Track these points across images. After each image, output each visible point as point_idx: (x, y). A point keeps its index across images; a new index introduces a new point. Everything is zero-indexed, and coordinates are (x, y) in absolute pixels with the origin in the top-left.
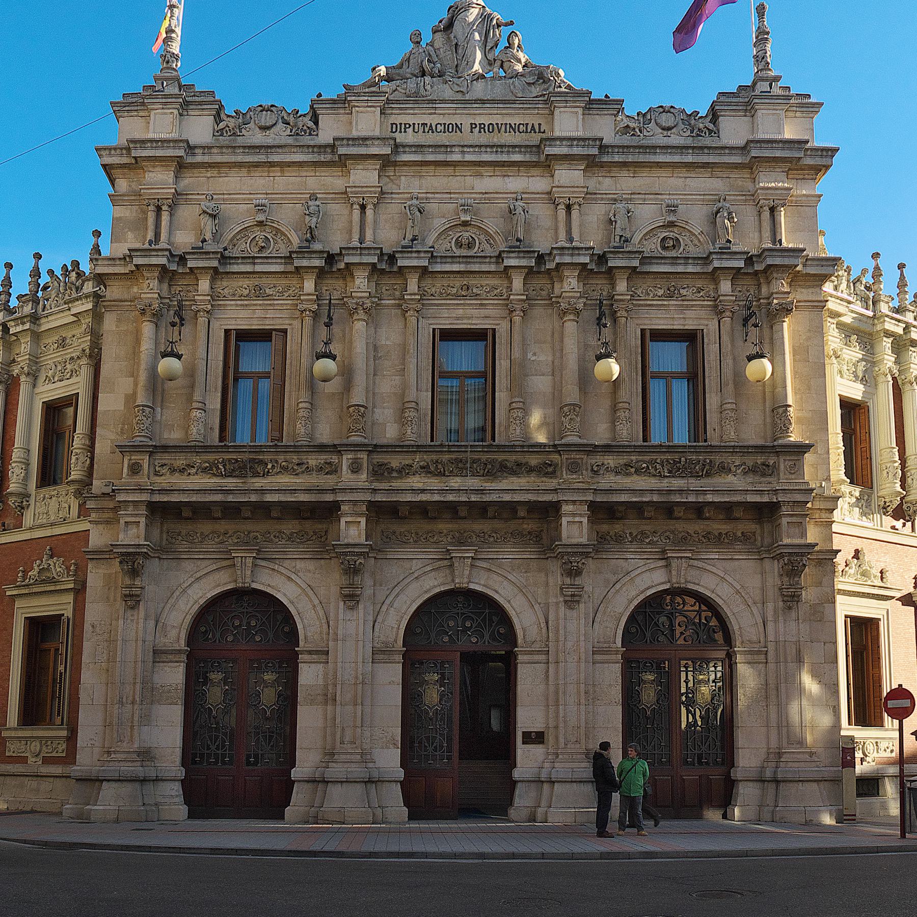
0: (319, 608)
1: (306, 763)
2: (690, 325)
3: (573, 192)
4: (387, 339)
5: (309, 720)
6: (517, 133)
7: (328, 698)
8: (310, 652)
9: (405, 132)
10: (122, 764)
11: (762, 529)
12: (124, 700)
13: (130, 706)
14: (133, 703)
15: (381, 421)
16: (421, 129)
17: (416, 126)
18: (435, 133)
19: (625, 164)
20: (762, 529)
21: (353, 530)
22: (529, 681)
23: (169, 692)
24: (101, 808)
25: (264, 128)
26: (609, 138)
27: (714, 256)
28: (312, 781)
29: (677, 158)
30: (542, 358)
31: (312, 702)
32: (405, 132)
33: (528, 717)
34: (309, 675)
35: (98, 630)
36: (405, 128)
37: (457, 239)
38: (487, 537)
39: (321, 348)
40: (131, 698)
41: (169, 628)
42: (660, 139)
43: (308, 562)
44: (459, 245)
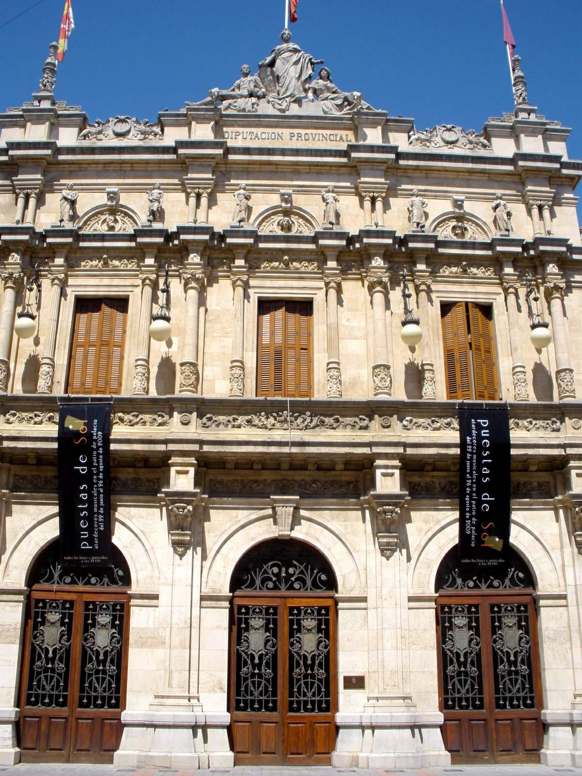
1: (137, 705)
2: (482, 299)
3: (376, 188)
4: (218, 305)
5: (141, 665)
6: (328, 141)
16: (249, 137)
17: (245, 133)
18: (260, 140)
21: (182, 481)
23: (8, 631)
25: (118, 135)
32: (235, 138)
33: (347, 664)
37: (279, 223)
39: (156, 310)
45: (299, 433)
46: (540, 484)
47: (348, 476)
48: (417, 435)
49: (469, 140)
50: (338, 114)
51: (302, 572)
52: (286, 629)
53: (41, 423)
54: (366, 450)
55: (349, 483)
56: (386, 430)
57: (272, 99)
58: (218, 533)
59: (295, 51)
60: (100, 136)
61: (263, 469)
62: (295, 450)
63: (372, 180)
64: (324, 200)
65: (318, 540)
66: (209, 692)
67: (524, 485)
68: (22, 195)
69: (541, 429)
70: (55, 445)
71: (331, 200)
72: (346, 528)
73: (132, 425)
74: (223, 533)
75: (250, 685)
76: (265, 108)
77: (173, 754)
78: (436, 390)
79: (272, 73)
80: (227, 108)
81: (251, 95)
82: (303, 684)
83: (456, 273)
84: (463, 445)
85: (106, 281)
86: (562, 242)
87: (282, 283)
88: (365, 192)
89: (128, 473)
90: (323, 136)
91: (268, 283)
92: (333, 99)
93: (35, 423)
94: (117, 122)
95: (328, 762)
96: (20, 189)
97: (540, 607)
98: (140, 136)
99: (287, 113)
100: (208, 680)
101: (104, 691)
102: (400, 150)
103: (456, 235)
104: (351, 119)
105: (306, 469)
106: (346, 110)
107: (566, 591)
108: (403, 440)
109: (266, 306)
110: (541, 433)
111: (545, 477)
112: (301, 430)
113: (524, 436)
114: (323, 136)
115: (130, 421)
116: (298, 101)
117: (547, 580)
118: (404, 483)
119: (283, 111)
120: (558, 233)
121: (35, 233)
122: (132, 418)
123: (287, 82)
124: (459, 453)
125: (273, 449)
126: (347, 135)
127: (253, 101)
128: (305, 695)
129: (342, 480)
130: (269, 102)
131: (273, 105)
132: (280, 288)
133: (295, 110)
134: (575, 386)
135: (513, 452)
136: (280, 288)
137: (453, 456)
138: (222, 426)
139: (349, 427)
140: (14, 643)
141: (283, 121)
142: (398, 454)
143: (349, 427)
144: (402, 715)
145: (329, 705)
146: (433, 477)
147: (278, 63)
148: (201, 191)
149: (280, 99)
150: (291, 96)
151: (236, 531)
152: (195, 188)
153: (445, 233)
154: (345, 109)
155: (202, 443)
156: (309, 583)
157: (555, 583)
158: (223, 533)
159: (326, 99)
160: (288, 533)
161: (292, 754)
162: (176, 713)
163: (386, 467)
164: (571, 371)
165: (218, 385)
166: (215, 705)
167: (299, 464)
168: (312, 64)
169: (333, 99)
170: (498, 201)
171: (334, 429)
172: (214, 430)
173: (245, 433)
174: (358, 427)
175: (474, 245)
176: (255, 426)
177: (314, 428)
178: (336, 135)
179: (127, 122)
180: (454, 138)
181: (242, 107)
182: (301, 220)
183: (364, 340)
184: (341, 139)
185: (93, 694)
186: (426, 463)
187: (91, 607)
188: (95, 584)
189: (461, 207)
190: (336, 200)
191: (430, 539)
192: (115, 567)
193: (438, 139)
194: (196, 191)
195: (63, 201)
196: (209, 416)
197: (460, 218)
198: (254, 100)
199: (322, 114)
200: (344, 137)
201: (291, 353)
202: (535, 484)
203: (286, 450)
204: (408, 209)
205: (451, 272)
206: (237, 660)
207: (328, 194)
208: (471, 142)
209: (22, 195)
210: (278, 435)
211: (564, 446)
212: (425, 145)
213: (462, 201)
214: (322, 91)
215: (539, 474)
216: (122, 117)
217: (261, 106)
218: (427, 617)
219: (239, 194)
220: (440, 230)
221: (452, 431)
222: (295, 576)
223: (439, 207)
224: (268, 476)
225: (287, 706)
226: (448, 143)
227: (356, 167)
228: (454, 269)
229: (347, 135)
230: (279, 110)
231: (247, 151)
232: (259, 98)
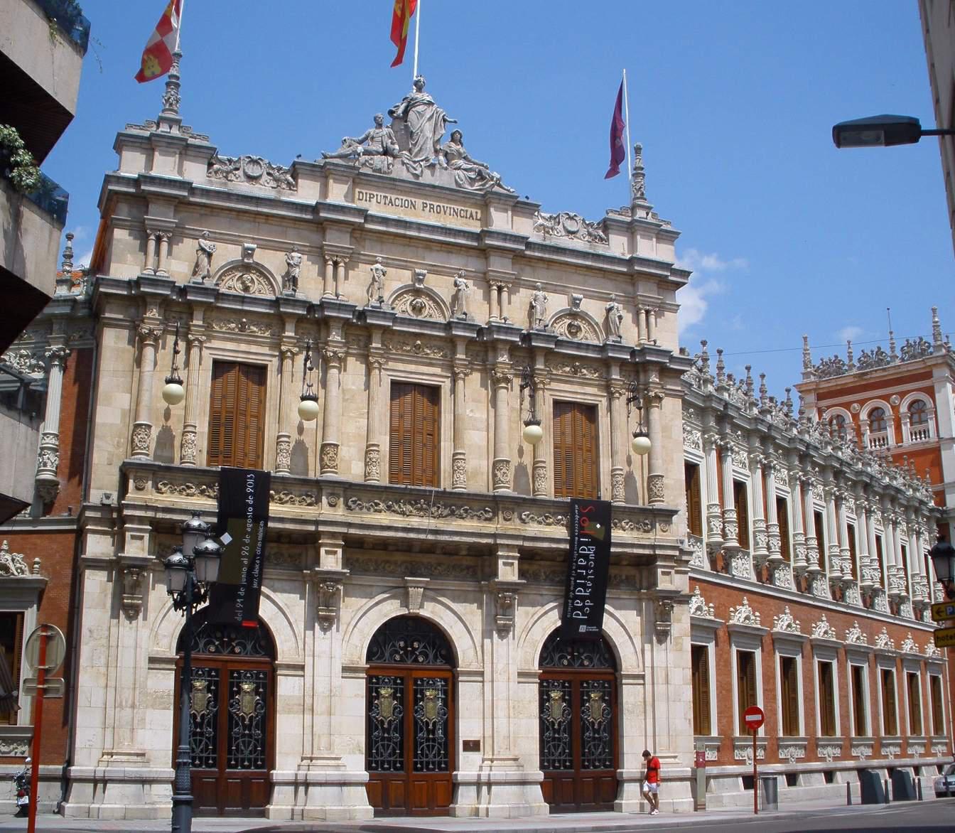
1: (284, 768)
2: (589, 400)
3: (504, 277)
4: (353, 384)
5: (287, 728)
7: (306, 708)
8: (289, 667)
9: (370, 201)
10: (126, 764)
11: (641, 573)
12: (124, 703)
13: (129, 710)
14: (133, 706)
15: (347, 458)
16: (383, 202)
17: (379, 197)
19: (541, 259)
20: (641, 573)
21: (331, 561)
22: (467, 692)
24: (109, 806)
25: (251, 178)
26: (535, 238)
27: (609, 347)
28: (295, 784)
29: (580, 262)
30: (478, 415)
32: (370, 201)
33: (467, 728)
34: (286, 687)
35: (95, 635)
36: (370, 198)
40: (130, 702)
41: (160, 637)
42: (566, 242)
43: (284, 583)
44: (414, 308)
45: (432, 521)
46: (627, 577)
47: (468, 561)
48: (533, 529)
49: (588, 231)
50: (469, 188)
51: (425, 647)
52: (411, 697)
53: (193, 495)
54: (490, 541)
55: (468, 568)
56: (508, 523)
57: (406, 161)
59: (430, 104)
60: (231, 177)
61: (397, 550)
62: (430, 537)
63: (499, 266)
64: (456, 285)
65: (442, 618)
66: (350, 753)
67: (615, 576)
68: (152, 237)
69: (635, 530)
70: (215, 520)
71: (462, 287)
73: (282, 503)
74: (359, 609)
75: (381, 747)
76: (400, 172)
77: (327, 808)
78: (547, 488)
79: (406, 126)
80: (364, 165)
81: (386, 152)
83: (569, 372)
84: (571, 542)
85: (243, 347)
86: (666, 353)
87: (412, 367)
88: (493, 280)
89: (272, 548)
90: (454, 211)
91: (400, 366)
92: (465, 170)
93: (188, 495)
94: (249, 162)
96: (151, 229)
97: (622, 684)
98: (273, 184)
99: (421, 180)
101: (251, 753)
102: (530, 240)
103: (570, 332)
104: (483, 196)
105: (434, 553)
106: (477, 185)
107: (644, 671)
108: (523, 534)
109: (398, 388)
110: (635, 534)
111: (632, 571)
112: (434, 517)
113: (623, 535)
114: (454, 211)
116: (432, 166)
117: (629, 659)
118: (522, 574)
119: (417, 176)
120: (664, 345)
121: (175, 286)
122: (282, 496)
123: (421, 142)
124: (568, 547)
125: (412, 535)
126: (476, 213)
127: (390, 162)
128: (427, 756)
129: (469, 566)
130: (403, 163)
131: (408, 169)
132: (411, 373)
133: (427, 178)
134: (665, 492)
135: (613, 550)
136: (411, 373)
137: (564, 550)
138: (365, 510)
139: (475, 518)
140: (168, 709)
141: (418, 189)
142: (517, 546)
143: (475, 518)
144: (513, 774)
145: (452, 764)
146: (540, 565)
147: (412, 115)
148: (339, 260)
149: (415, 162)
150: (427, 160)
152: (333, 255)
153: (561, 330)
154: (477, 184)
155: (350, 525)
156: (431, 656)
157: (635, 664)
158: (359, 609)
159: (459, 168)
160: (418, 611)
161: (416, 807)
162: (328, 772)
163: (508, 557)
164: (662, 477)
165: (351, 468)
166: (356, 767)
167: (429, 548)
168: (445, 120)
169: (465, 170)
170: (612, 304)
171: (463, 518)
172: (358, 514)
173: (385, 518)
174: (483, 518)
175: (588, 347)
176: (394, 511)
177: (446, 516)
178: (467, 211)
179: (259, 163)
180: (574, 229)
181: (379, 167)
182: (430, 302)
183: (489, 433)
184: (471, 216)
185: (240, 756)
186: (537, 554)
187: (235, 675)
188: (240, 653)
189: (577, 305)
190: (466, 286)
191: (536, 622)
192: (264, 640)
193: (560, 227)
194: (335, 259)
195: (200, 253)
196: (354, 499)
197: (574, 315)
198: (390, 159)
199: (454, 186)
200: (474, 214)
201: (418, 437)
202: (624, 577)
203: (422, 536)
204: (531, 303)
205: (565, 372)
206: (371, 725)
207: (460, 280)
208: (590, 234)
209: (152, 237)
210: (415, 521)
211: (653, 547)
212: (548, 232)
213: (580, 300)
214: (453, 157)
215: (628, 568)
216: (254, 157)
217: (395, 167)
218: (533, 690)
219: (377, 269)
220: (557, 326)
221: (561, 527)
222: (419, 650)
223: (557, 303)
224: (399, 557)
225: (411, 766)
226: (570, 233)
227: (484, 250)
228: (568, 369)
229: (476, 213)
230: (413, 174)
231: (385, 221)
232: (394, 157)
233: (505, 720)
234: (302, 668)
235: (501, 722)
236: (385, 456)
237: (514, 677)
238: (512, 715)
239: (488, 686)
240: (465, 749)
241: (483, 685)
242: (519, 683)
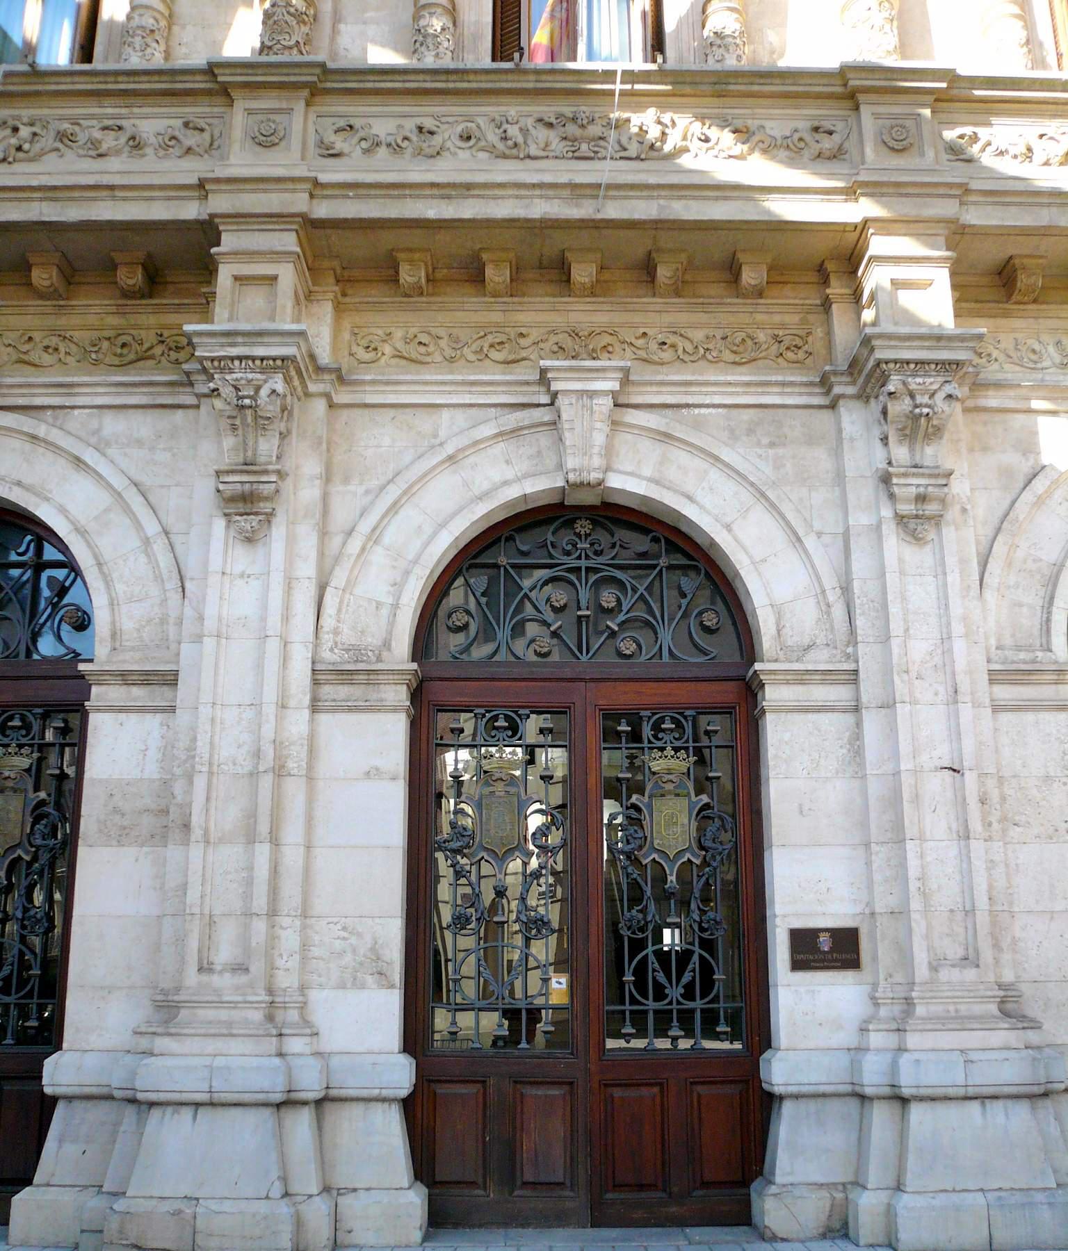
0: (160, 546)
8: (125, 678)
22: (799, 761)
31: (123, 836)
33: (804, 884)
34: (116, 749)
38: (654, 346)
58: (375, 483)
66: (342, 986)
72: (778, 465)
82: (652, 958)
95: (741, 1216)
100: (338, 945)
115: (95, 143)
128: (660, 994)
138: (382, 152)
151: (425, 465)
233: (952, 850)
234: (170, 679)
235: (934, 856)
236: (476, 37)
237: (973, 680)
238: (976, 825)
239: (872, 723)
240: (798, 965)
241: (859, 724)
242: (997, 709)
